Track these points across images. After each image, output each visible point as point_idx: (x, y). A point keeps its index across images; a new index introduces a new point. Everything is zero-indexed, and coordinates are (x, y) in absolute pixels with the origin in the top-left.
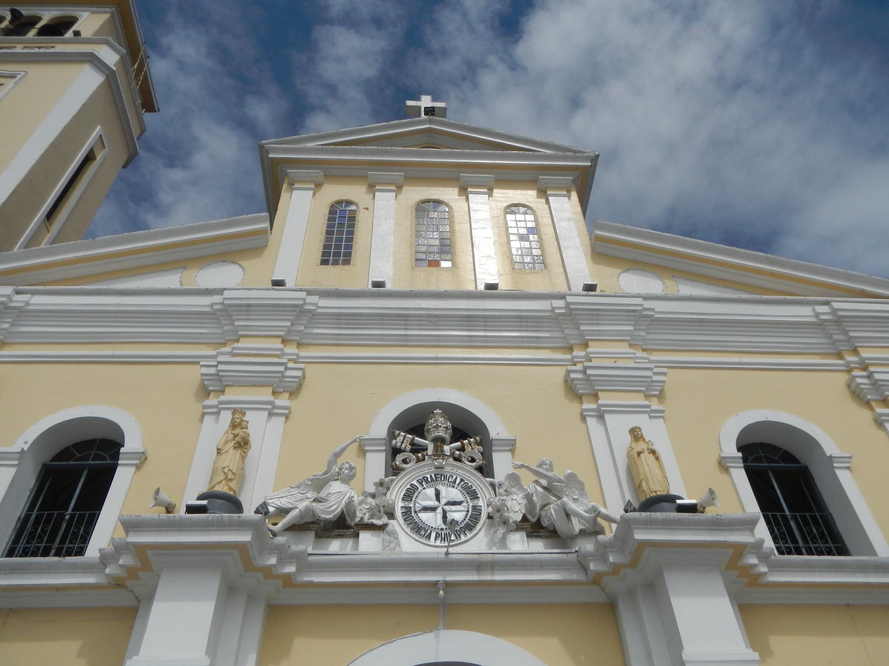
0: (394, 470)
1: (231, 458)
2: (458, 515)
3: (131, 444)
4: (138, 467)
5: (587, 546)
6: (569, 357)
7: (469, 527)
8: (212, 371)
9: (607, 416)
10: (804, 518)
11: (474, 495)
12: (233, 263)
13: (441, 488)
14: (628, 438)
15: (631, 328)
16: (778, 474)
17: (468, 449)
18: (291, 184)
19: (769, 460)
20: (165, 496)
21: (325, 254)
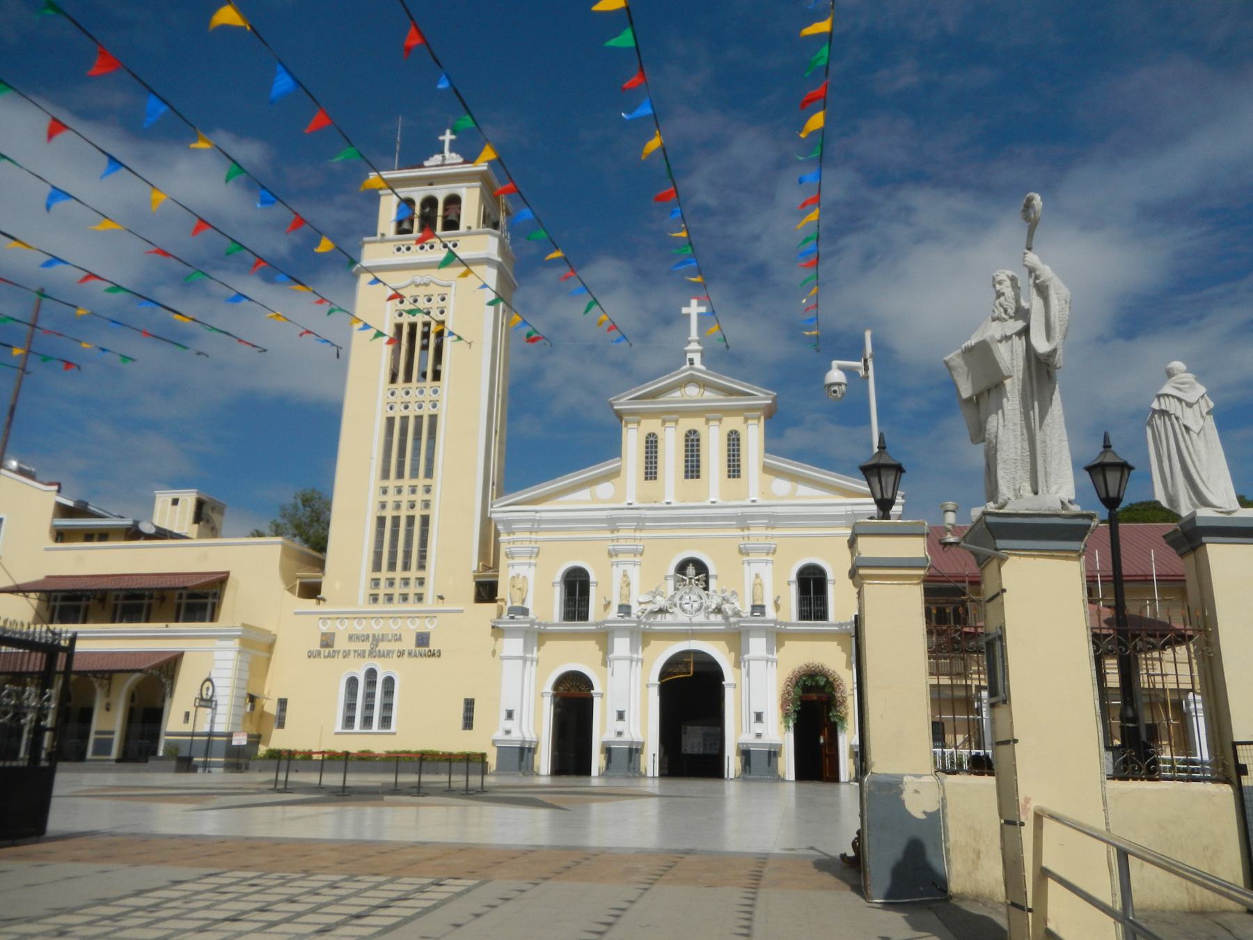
0: (676, 589)
1: (625, 591)
2: (696, 605)
3: (592, 579)
4: (596, 586)
5: (732, 620)
6: (741, 533)
7: (699, 610)
8: (612, 548)
9: (751, 564)
10: (817, 598)
11: (701, 598)
12: (609, 481)
13: (691, 596)
14: (755, 576)
15: (767, 521)
16: (815, 580)
17: (701, 579)
18: (627, 423)
19: (815, 574)
20: (608, 599)
21: (646, 473)
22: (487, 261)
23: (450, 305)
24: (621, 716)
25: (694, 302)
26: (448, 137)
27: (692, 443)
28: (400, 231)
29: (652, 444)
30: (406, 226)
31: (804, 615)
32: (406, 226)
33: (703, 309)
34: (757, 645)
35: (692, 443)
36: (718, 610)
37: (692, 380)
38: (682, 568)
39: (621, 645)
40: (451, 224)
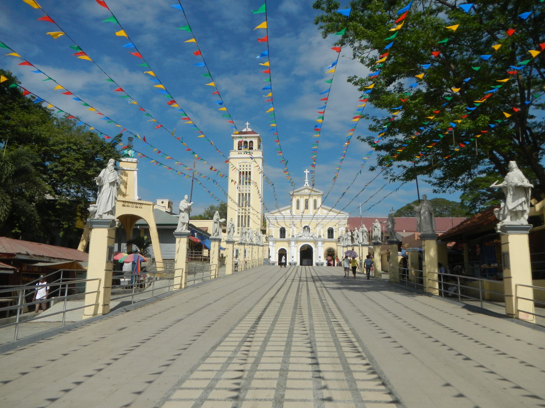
22: (260, 158)
23: (252, 167)
24: (293, 257)
25: (307, 170)
26: (247, 124)
27: (307, 202)
28: (239, 149)
29: (298, 202)
30: (240, 148)
31: (329, 237)
32: (240, 148)
33: (309, 172)
34: (320, 244)
35: (307, 202)
36: (312, 236)
37: (307, 188)
38: (305, 228)
39: (293, 243)
40: (251, 148)
